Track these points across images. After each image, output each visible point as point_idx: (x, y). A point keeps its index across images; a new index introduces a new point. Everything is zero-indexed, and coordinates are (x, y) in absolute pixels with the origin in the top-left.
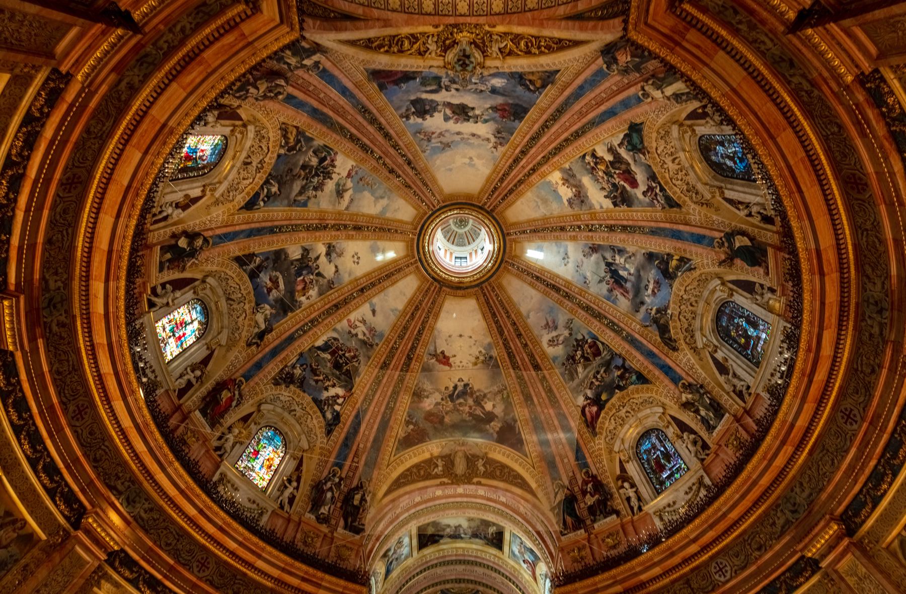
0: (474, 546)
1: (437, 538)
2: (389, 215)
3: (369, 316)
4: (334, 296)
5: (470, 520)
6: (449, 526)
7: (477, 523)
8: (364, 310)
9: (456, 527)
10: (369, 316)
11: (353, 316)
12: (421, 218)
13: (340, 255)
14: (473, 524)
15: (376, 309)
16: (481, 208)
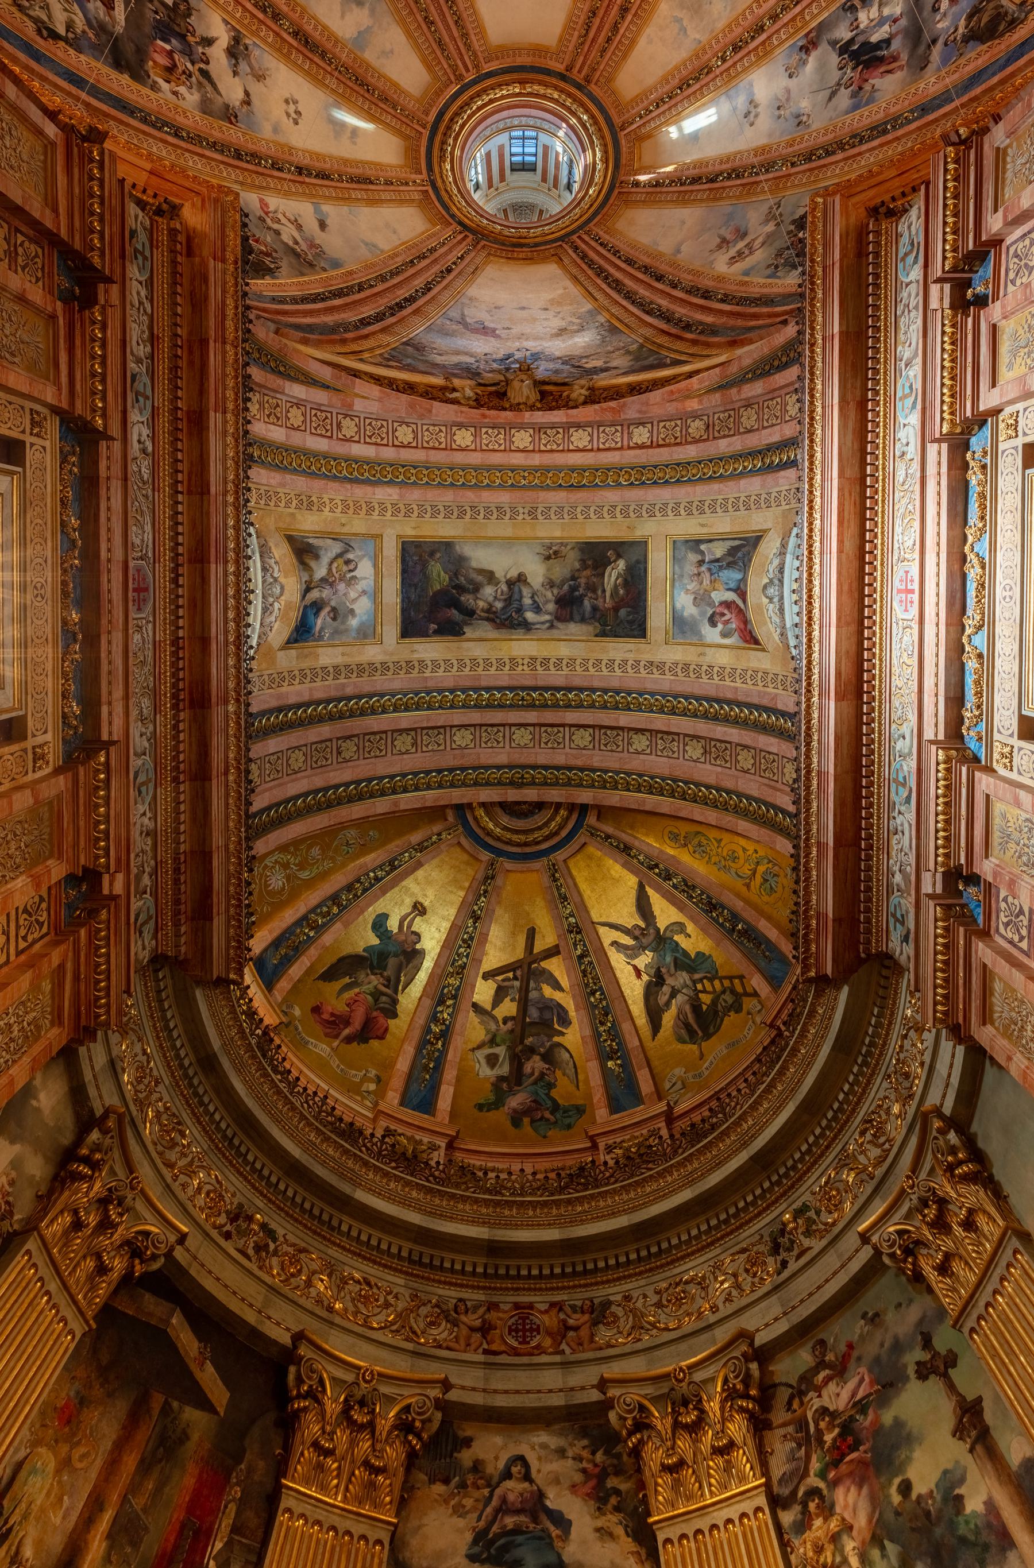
0: (564, 650)
1: (454, 614)
2: (369, 56)
3: (311, 224)
4: (232, 135)
5: (551, 554)
6: (490, 576)
7: (572, 560)
8: (303, 209)
9: (510, 583)
10: (311, 224)
11: (274, 202)
12: (439, 93)
13: (260, 77)
14: (560, 571)
15: (328, 222)
16: (563, 77)
